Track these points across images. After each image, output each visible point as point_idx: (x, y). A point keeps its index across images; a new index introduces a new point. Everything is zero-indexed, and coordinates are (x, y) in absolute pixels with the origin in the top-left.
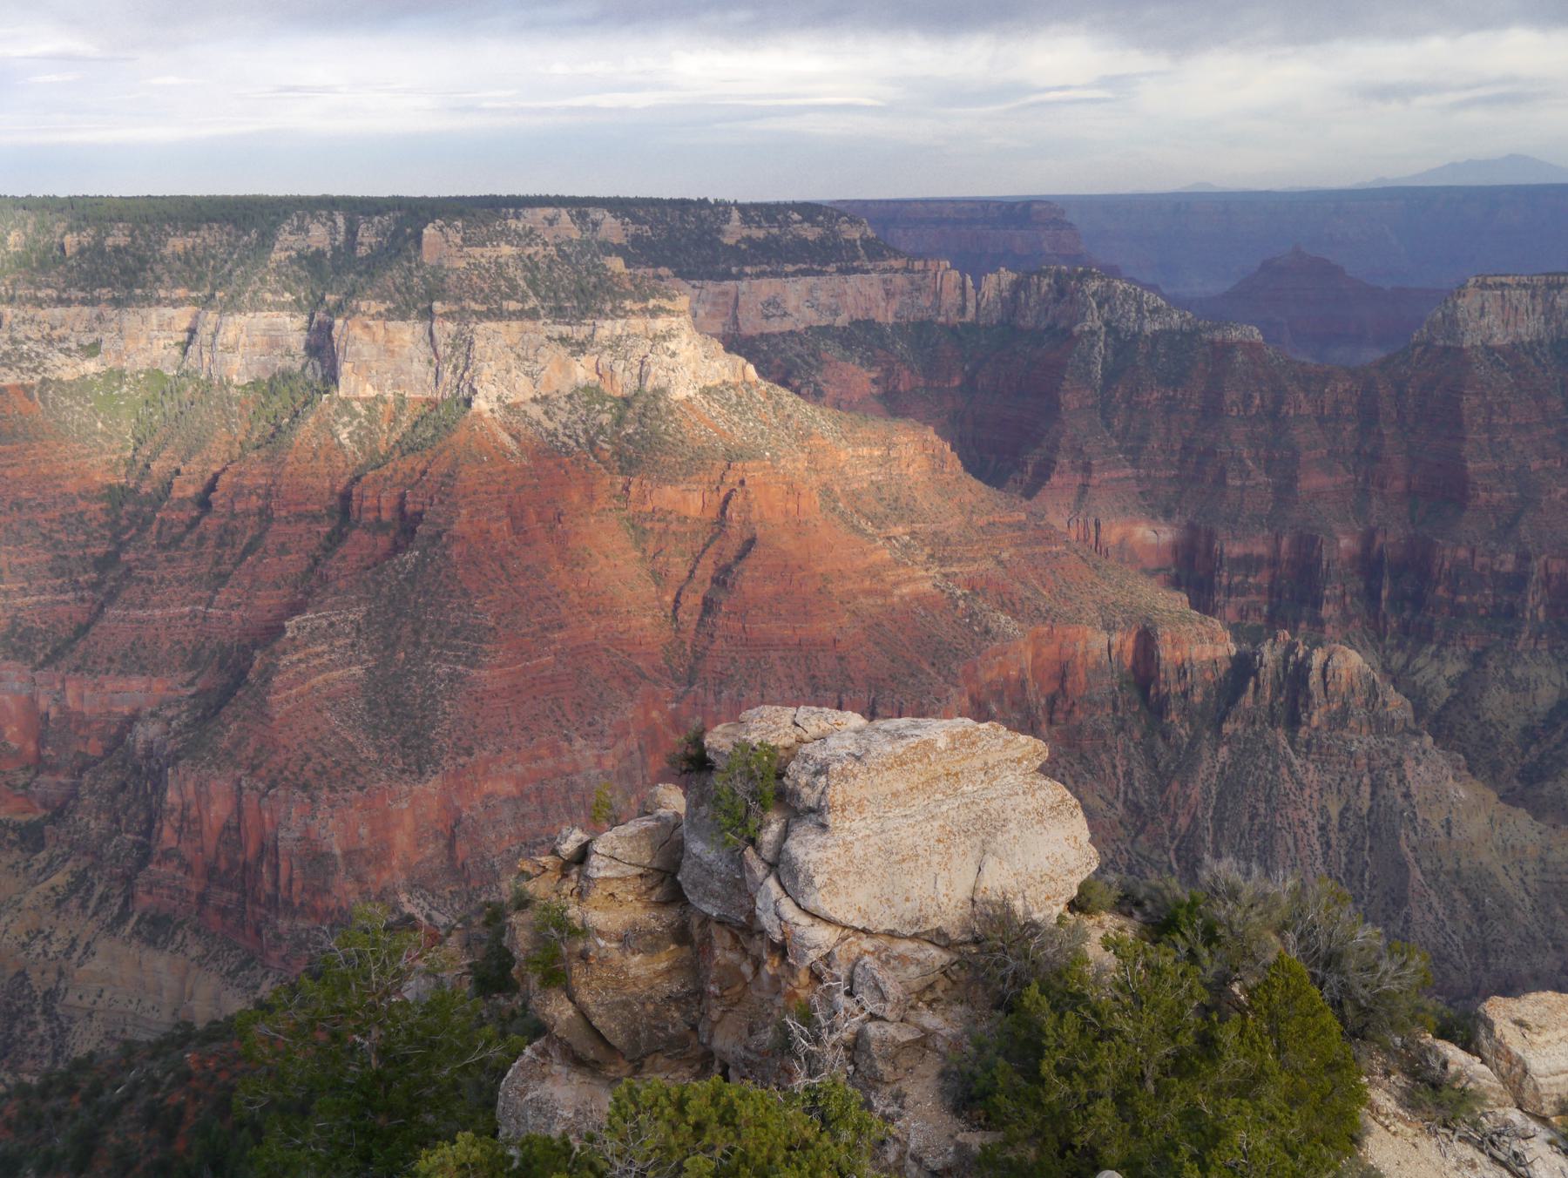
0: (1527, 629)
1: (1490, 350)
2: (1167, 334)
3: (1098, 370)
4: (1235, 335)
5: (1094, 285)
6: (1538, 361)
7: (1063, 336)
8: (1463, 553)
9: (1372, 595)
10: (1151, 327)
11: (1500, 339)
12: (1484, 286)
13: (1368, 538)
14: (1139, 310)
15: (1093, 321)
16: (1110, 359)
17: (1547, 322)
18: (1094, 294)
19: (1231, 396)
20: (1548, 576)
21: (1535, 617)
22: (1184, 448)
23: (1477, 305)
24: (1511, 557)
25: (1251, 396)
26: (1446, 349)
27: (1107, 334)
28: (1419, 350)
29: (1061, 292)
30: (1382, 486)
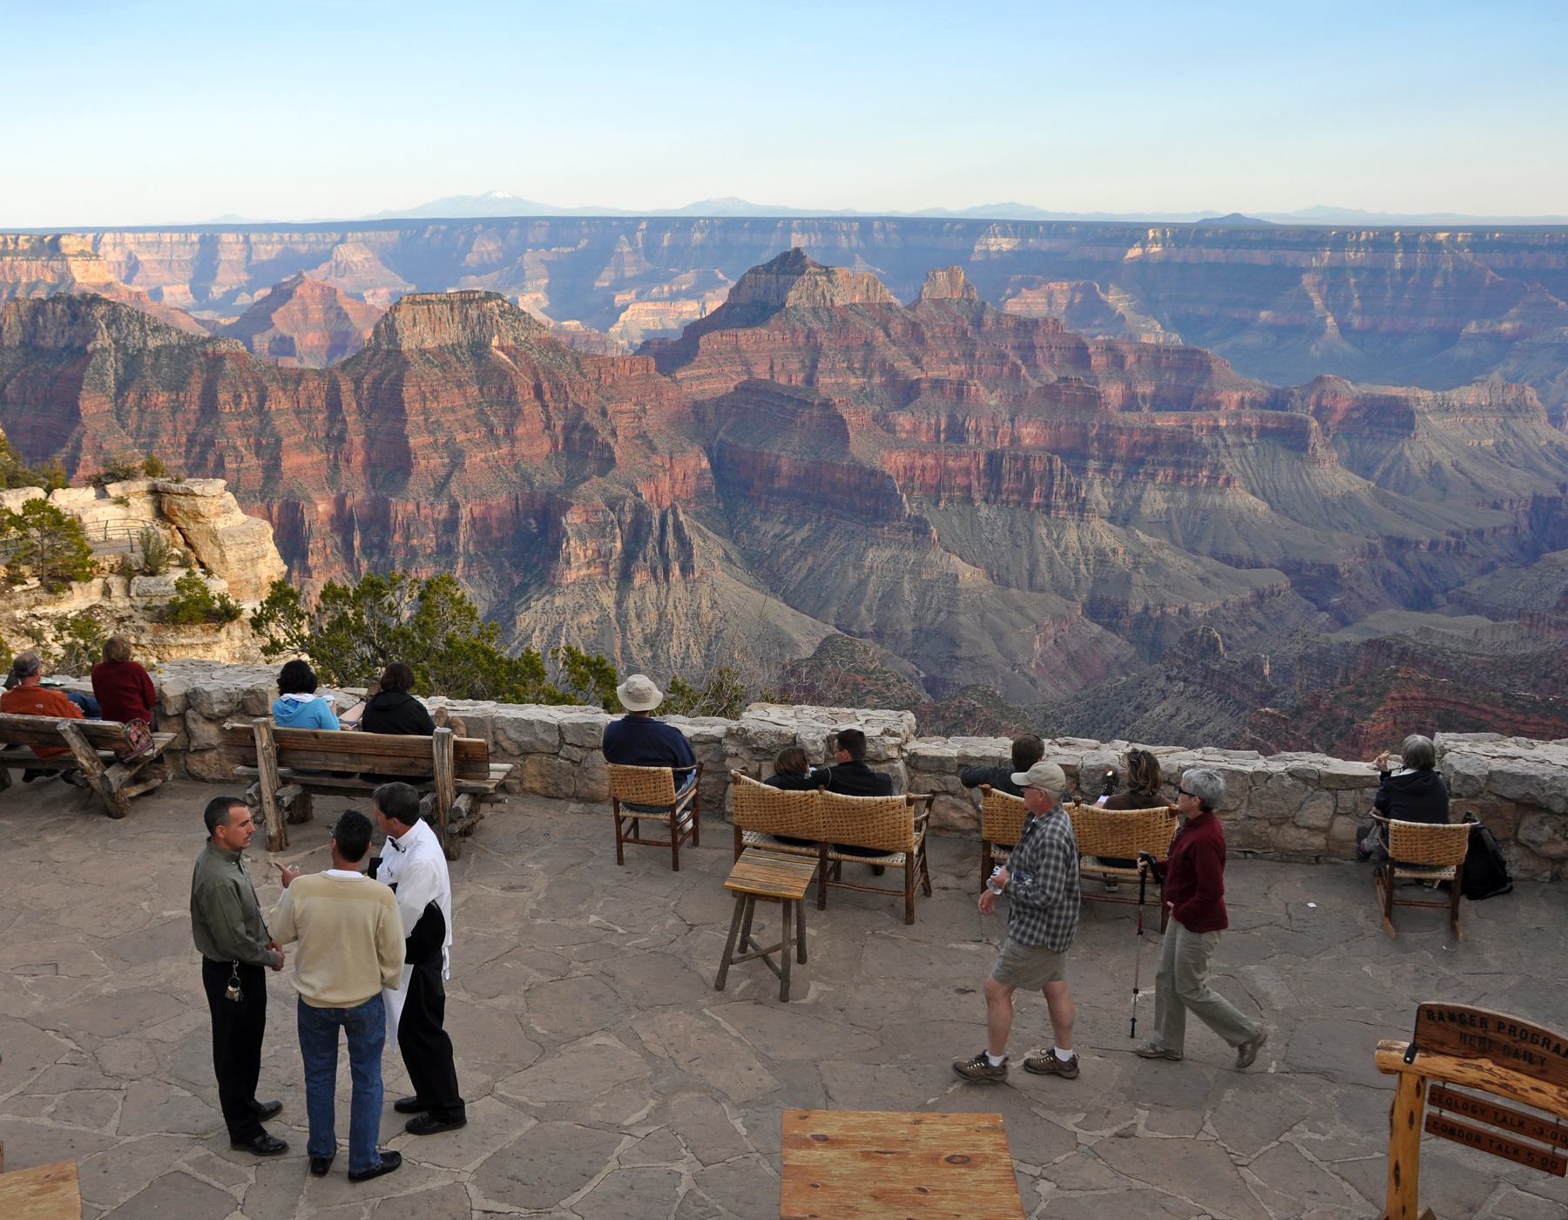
0: (461, 560)
1: (422, 352)
2: (168, 347)
3: (111, 381)
4: (223, 347)
5: (100, 310)
6: (458, 359)
7: (78, 353)
8: (411, 507)
9: (348, 546)
10: (153, 343)
11: (429, 344)
12: (414, 302)
13: (340, 502)
14: (142, 328)
15: (103, 339)
16: (121, 371)
17: (464, 329)
18: (102, 317)
19: (224, 397)
20: (473, 518)
21: (466, 551)
22: (188, 440)
23: (410, 317)
24: (445, 507)
25: (240, 396)
26: (389, 352)
27: (117, 350)
28: (369, 353)
29: (75, 316)
30: (348, 461)
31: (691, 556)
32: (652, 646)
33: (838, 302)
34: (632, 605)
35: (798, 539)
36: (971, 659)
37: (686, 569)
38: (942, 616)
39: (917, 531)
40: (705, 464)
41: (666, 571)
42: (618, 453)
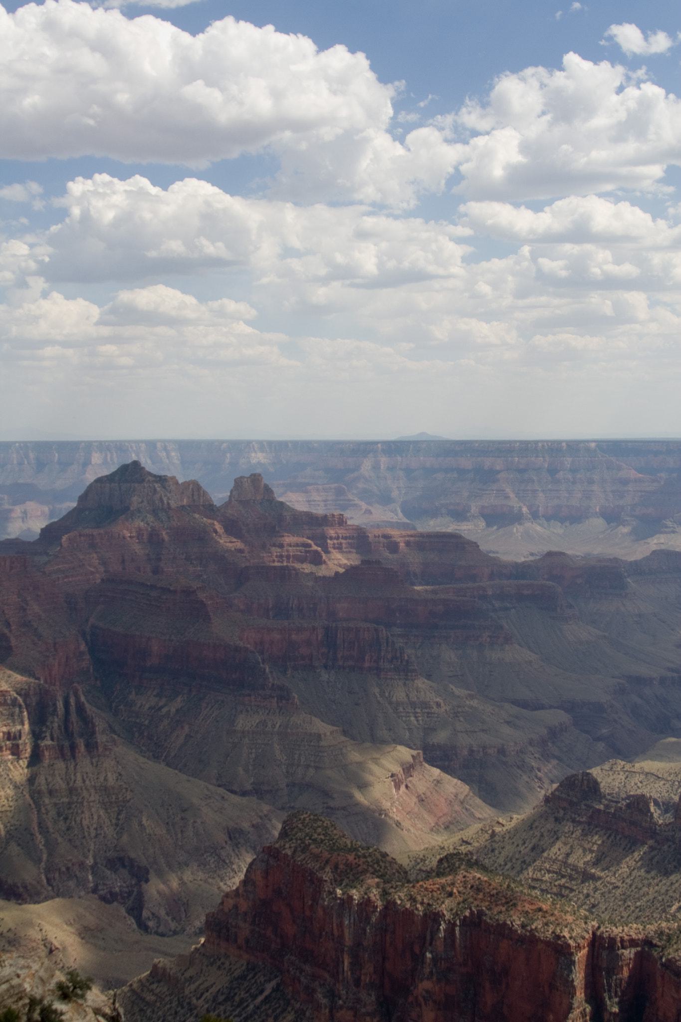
31: (93, 733)
32: (66, 819)
33: (173, 504)
34: (43, 782)
35: (173, 710)
36: (344, 808)
37: (91, 747)
38: (312, 771)
39: (281, 698)
40: (83, 647)
41: (73, 748)
42: (13, 642)
